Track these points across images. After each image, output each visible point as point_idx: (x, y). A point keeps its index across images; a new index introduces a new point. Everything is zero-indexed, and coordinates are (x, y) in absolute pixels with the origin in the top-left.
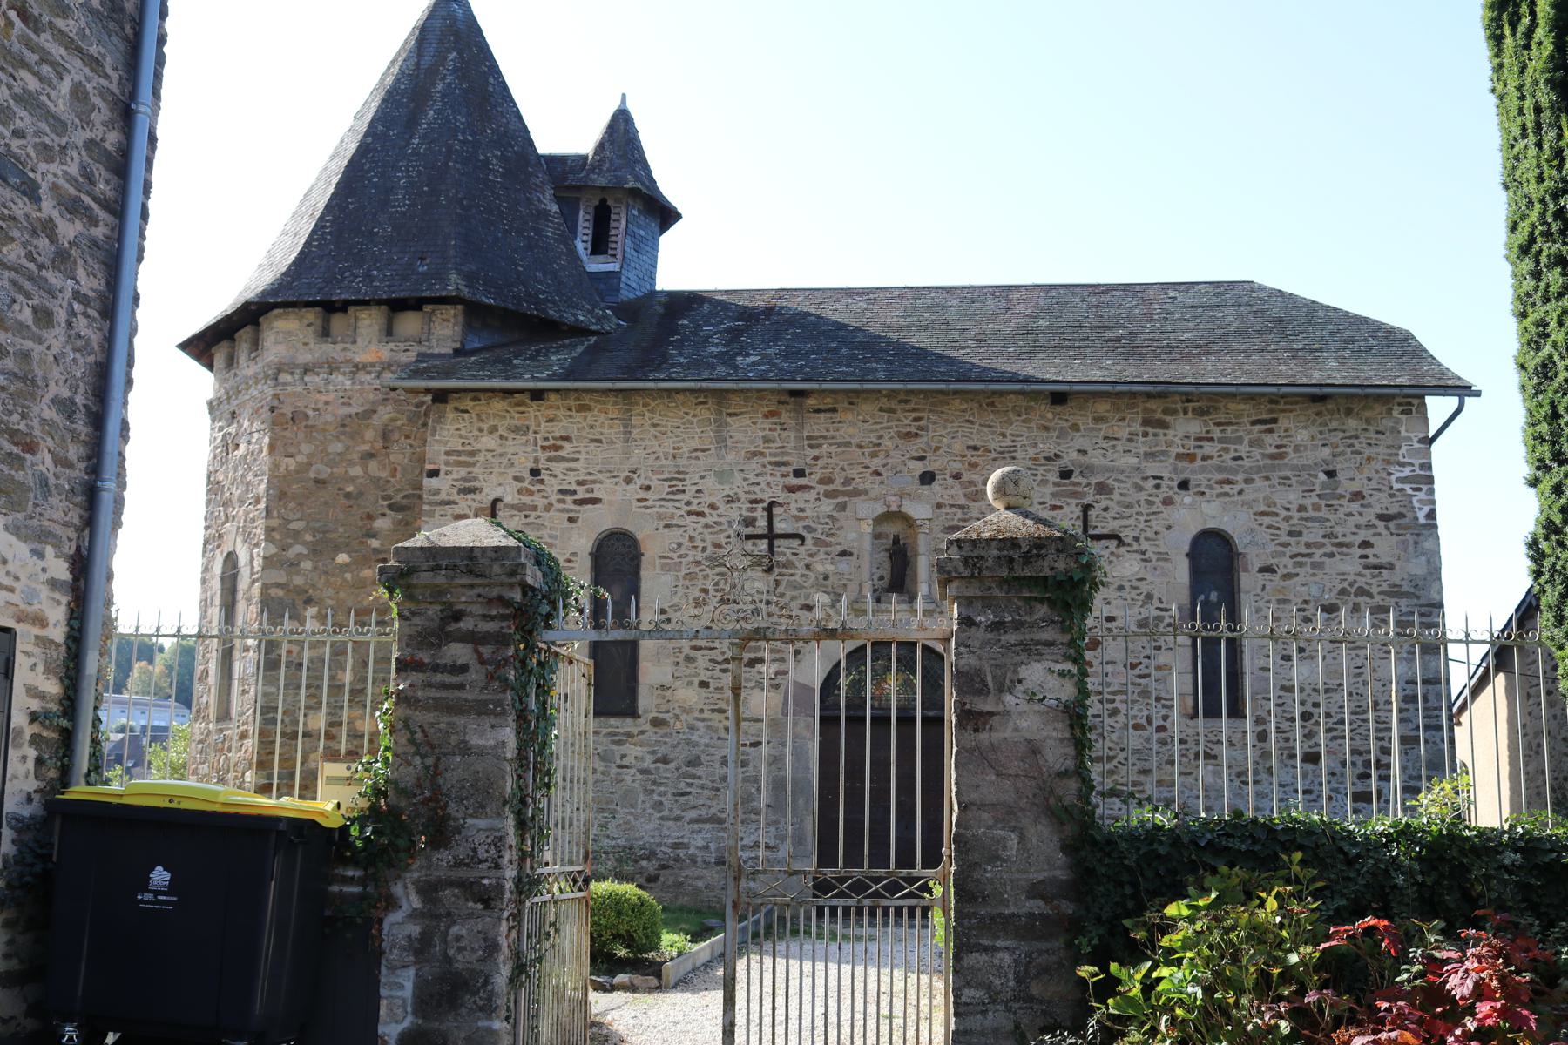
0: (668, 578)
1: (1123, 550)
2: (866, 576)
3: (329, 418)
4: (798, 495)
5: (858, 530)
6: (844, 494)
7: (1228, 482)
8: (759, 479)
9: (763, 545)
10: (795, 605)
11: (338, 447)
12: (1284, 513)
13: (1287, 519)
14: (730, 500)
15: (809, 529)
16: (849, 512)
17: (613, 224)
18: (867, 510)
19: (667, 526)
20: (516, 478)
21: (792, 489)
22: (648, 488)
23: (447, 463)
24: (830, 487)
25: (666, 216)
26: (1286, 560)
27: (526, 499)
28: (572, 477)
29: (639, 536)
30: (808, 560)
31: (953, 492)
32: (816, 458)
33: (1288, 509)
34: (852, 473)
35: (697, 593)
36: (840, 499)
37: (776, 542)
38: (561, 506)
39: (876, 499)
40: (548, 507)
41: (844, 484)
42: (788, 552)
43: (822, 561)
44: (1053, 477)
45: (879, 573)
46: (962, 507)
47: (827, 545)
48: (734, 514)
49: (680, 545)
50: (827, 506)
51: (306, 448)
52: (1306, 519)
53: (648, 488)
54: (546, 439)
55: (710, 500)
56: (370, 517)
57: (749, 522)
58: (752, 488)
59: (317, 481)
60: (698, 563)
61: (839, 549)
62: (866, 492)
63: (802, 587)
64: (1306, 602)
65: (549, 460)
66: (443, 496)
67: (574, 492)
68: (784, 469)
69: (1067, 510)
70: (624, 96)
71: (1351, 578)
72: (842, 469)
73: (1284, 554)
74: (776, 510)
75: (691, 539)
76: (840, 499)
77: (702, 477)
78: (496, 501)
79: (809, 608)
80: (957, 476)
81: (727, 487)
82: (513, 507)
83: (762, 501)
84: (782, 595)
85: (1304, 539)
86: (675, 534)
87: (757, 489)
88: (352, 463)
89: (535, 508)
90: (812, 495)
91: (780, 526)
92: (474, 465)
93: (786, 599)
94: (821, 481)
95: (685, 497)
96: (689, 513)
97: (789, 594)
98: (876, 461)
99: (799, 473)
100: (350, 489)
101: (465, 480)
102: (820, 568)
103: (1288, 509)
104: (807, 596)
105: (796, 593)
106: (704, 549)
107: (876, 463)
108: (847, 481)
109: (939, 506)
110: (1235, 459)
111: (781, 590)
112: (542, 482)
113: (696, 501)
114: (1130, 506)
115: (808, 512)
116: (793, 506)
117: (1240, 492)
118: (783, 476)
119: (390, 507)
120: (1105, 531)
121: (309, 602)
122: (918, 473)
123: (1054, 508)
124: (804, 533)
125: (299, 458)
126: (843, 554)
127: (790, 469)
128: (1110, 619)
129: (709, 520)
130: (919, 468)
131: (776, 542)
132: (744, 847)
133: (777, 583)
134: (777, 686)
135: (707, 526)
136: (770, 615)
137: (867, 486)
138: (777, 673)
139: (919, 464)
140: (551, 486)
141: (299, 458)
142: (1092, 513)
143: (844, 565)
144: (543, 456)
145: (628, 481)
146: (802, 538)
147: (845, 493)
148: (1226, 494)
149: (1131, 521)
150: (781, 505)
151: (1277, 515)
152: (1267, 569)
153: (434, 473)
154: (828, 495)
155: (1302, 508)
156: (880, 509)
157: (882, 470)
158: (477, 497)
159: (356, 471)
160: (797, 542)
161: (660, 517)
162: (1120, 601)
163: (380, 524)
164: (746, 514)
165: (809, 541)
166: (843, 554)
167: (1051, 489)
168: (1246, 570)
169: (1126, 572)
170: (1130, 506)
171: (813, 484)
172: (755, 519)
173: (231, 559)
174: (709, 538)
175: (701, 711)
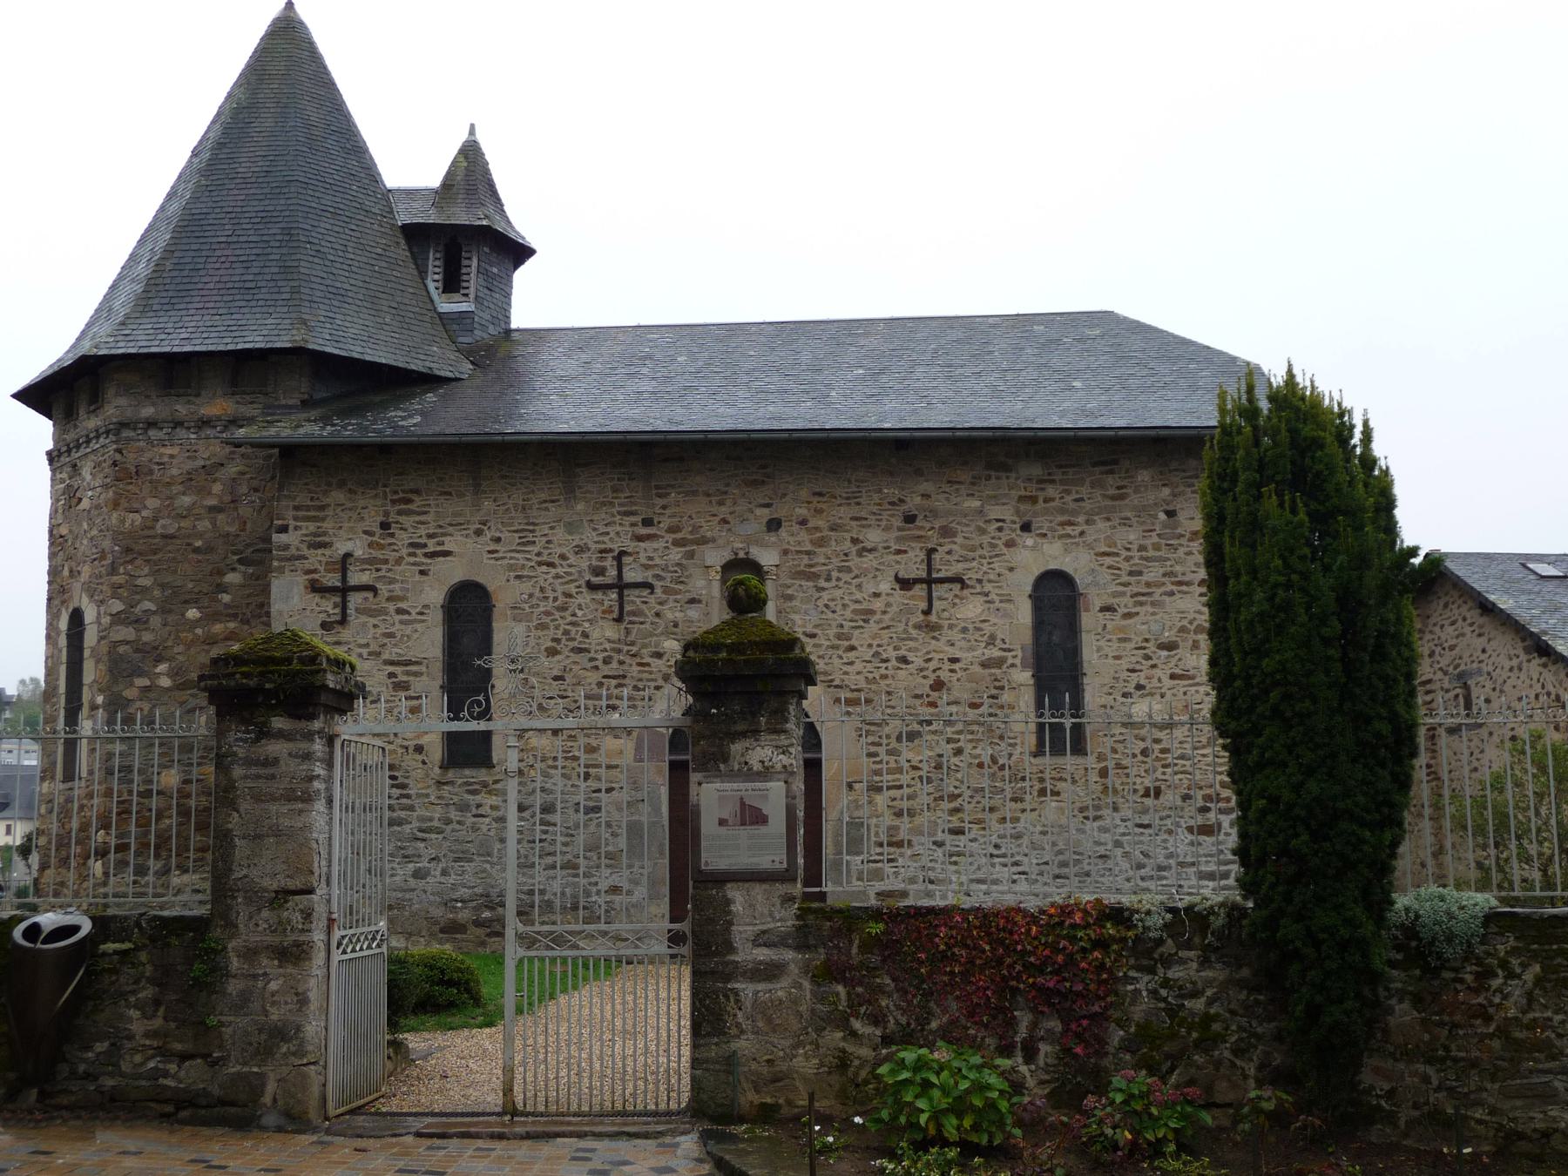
0: (519, 629)
1: (966, 592)
3: (175, 472)
7: (1071, 524)
8: (609, 529)
11: (187, 500)
12: (1124, 553)
13: (1127, 559)
14: (580, 550)
15: (657, 577)
17: (465, 262)
18: (716, 557)
19: (518, 577)
20: (366, 532)
21: (640, 538)
22: (498, 540)
23: (296, 519)
24: (679, 536)
25: (519, 253)
26: (1127, 600)
27: (379, 554)
28: (423, 531)
29: (490, 588)
32: (664, 507)
33: (1128, 549)
35: (550, 644)
37: (626, 592)
38: (412, 559)
40: (399, 561)
41: (691, 533)
42: (638, 601)
46: (808, 553)
47: (677, 592)
48: (585, 565)
49: (531, 596)
50: (676, 554)
51: (153, 503)
52: (1147, 559)
53: (498, 540)
54: (396, 492)
55: (559, 551)
56: (221, 573)
57: (599, 571)
59: (164, 536)
60: (547, 613)
61: (689, 596)
62: (713, 540)
63: (652, 635)
64: (1147, 640)
65: (400, 513)
66: (293, 551)
67: (425, 546)
68: (633, 519)
69: (911, 554)
70: (472, 126)
71: (1191, 616)
73: (1123, 594)
74: (626, 560)
75: (542, 589)
77: (552, 528)
78: (348, 555)
79: (659, 655)
80: (803, 522)
81: (576, 537)
82: (364, 561)
83: (611, 550)
85: (1144, 578)
86: (526, 587)
87: (606, 539)
88: (199, 518)
89: (386, 561)
90: (659, 544)
91: (630, 576)
92: (323, 519)
93: (634, 649)
94: (671, 530)
95: (536, 549)
96: (540, 564)
100: (198, 543)
101: (315, 535)
102: (670, 616)
103: (1128, 549)
106: (555, 599)
109: (786, 552)
110: (1077, 500)
111: (631, 638)
112: (392, 535)
113: (546, 552)
114: (973, 549)
115: (658, 561)
116: (642, 555)
117: (1082, 533)
118: (632, 525)
119: (240, 561)
120: (949, 574)
121: (159, 660)
122: (765, 521)
123: (899, 552)
124: (655, 582)
125: (145, 513)
126: (692, 601)
127: (638, 519)
128: (954, 660)
129: (560, 570)
131: (626, 592)
133: (628, 632)
135: (557, 576)
136: (621, 663)
139: (766, 511)
140: (403, 538)
141: (145, 513)
142: (936, 556)
144: (393, 509)
145: (478, 533)
146: (650, 586)
148: (1069, 536)
149: (974, 564)
150: (630, 554)
151: (1117, 555)
152: (1107, 609)
153: (284, 529)
154: (676, 543)
155: (1142, 548)
156: (727, 556)
157: (729, 518)
158: (327, 552)
159: (203, 525)
160: (646, 592)
161: (511, 568)
162: (963, 643)
163: (232, 578)
164: (595, 563)
165: (658, 591)
166: (692, 601)
168: (1087, 610)
169: (970, 615)
170: (973, 549)
173: (77, 617)
174: (560, 589)
175: (555, 759)
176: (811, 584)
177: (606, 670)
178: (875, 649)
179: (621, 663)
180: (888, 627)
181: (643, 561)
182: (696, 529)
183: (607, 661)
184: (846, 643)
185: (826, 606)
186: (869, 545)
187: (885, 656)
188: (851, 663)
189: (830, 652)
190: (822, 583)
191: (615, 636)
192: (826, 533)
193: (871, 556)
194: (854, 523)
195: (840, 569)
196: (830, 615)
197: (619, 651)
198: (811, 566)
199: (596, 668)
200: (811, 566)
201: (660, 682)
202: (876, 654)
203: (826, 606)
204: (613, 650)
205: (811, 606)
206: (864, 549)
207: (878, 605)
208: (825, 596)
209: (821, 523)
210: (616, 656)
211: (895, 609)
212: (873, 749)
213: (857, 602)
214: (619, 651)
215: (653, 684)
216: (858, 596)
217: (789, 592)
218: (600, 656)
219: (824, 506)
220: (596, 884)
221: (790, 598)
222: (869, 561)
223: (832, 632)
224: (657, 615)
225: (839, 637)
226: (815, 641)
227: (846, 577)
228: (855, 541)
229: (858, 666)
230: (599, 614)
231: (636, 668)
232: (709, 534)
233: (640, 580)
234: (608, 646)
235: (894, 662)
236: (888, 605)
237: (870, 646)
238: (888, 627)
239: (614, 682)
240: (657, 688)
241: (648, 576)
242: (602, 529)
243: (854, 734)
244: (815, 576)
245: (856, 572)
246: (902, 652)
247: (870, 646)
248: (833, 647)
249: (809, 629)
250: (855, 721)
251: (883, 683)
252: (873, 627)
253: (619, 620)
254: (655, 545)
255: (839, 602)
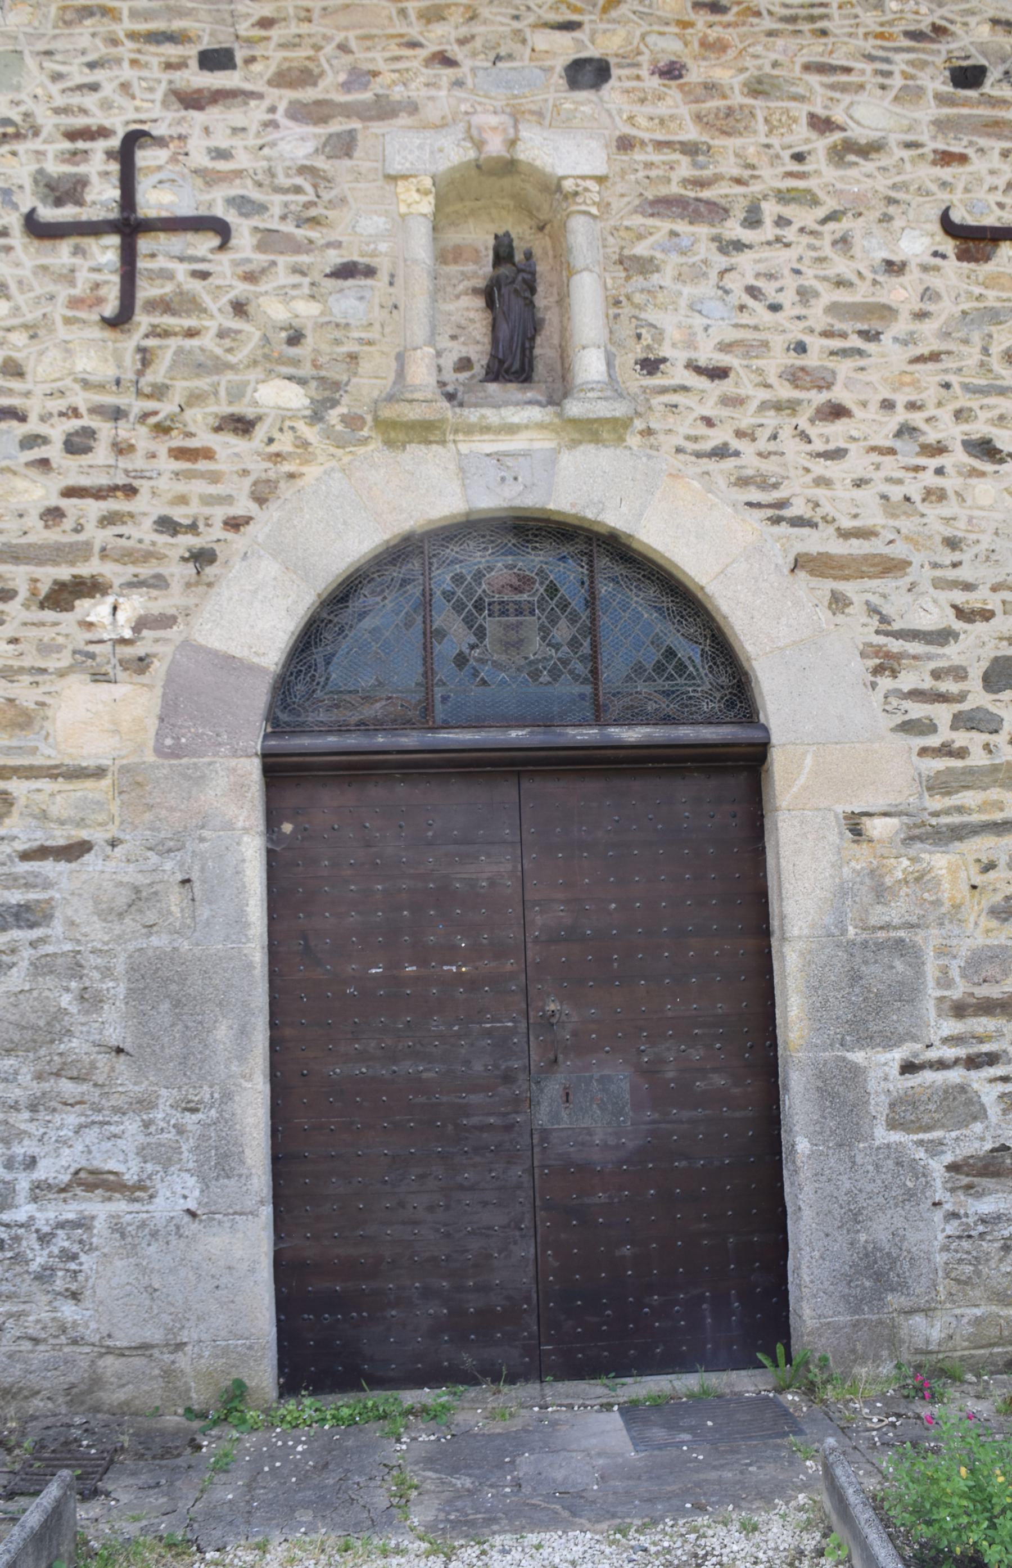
2: (419, 331)
4: (213, 115)
5: (391, 210)
6: (346, 119)
8: (98, 75)
9: (106, 251)
10: (199, 420)
15: (243, 205)
16: (362, 160)
18: (423, 152)
21: (192, 101)
24: (308, 94)
30: (241, 289)
31: (662, 109)
34: (377, 59)
36: (337, 126)
39: (441, 126)
41: (346, 87)
42: (181, 270)
43: (284, 294)
44: (936, 82)
45: (455, 351)
46: (690, 149)
47: (297, 247)
50: (298, 144)
57: (67, 191)
58: (75, 100)
61: (335, 258)
62: (413, 108)
63: (220, 366)
68: (172, 51)
69: (978, 165)
72: (343, 48)
74: (145, 157)
76: (337, 126)
79: (242, 425)
80: (672, 72)
83: (103, 133)
84: (159, 392)
87: (89, 101)
90: (256, 113)
93: (166, 408)
94: (282, 79)
97: (181, 388)
98: (439, 30)
99: (215, 59)
102: (277, 311)
104: (236, 393)
105: (203, 383)
107: (440, 36)
108: (360, 77)
109: (625, 144)
111: (157, 374)
115: (242, 160)
118: (169, 66)
122: (560, 63)
123: (946, 158)
124: (231, 217)
126: (346, 271)
127: (191, 52)
130: (565, 47)
132: (39, 1191)
133: (146, 357)
134: (142, 664)
136: (122, 449)
137: (416, 91)
138: (140, 625)
139: (564, 39)
143: (348, 302)
146: (222, 230)
147: (348, 111)
150: (160, 142)
154: (300, 113)
156: (453, 153)
160: (205, 243)
164: (55, 168)
165: (243, 238)
166: (346, 271)
167: (929, 111)
171: (258, 86)
172: (81, 183)
176: (703, 231)
177: (73, 470)
178: (902, 415)
179: (122, 449)
180: (934, 357)
181: (200, 159)
182: (360, 77)
183: (78, 444)
184: (819, 398)
185: (752, 291)
186: (861, 135)
187: (931, 436)
188: (837, 454)
189: (771, 420)
190: (734, 229)
191: (108, 372)
192: (738, 99)
193: (869, 166)
194: (814, 79)
195: (783, 197)
196: (768, 317)
197: (117, 414)
198: (701, 183)
199: (44, 463)
200: (701, 183)
201: (244, 506)
202: (905, 431)
203: (752, 291)
204: (96, 410)
205: (706, 289)
206: (850, 147)
207: (901, 293)
208: (743, 260)
209: (722, 75)
210: (105, 429)
211: (946, 309)
212: (917, 710)
213: (840, 283)
214: (117, 414)
215: (220, 513)
216: (841, 266)
217: (641, 249)
218: (58, 431)
219: (731, 35)
220: (31, 1163)
221: (645, 266)
222: (862, 178)
223: (777, 360)
224: (239, 308)
225: (795, 377)
226: (725, 387)
227: (804, 216)
228: (822, 124)
229: (857, 463)
230: (59, 311)
231: (168, 465)
232: (398, 93)
233: (186, 209)
234: (81, 399)
235: (958, 457)
236: (928, 294)
237: (888, 405)
238: (934, 357)
239: (94, 508)
240: (234, 524)
241: (216, 203)
242: (80, 76)
243: (860, 667)
244: (717, 211)
245: (831, 204)
246: (979, 428)
247: (888, 405)
248: (778, 407)
249: (707, 355)
250: (861, 629)
251: (933, 512)
252: (889, 354)
253: (120, 320)
254: (236, 116)
255: (791, 283)
